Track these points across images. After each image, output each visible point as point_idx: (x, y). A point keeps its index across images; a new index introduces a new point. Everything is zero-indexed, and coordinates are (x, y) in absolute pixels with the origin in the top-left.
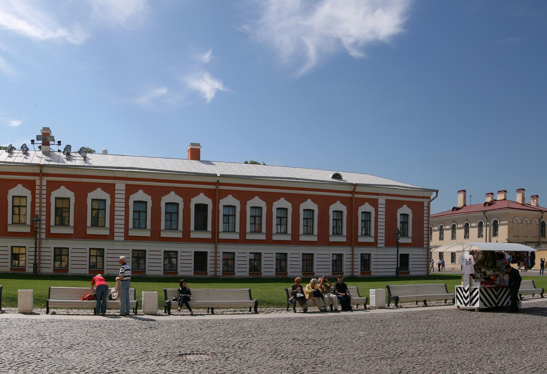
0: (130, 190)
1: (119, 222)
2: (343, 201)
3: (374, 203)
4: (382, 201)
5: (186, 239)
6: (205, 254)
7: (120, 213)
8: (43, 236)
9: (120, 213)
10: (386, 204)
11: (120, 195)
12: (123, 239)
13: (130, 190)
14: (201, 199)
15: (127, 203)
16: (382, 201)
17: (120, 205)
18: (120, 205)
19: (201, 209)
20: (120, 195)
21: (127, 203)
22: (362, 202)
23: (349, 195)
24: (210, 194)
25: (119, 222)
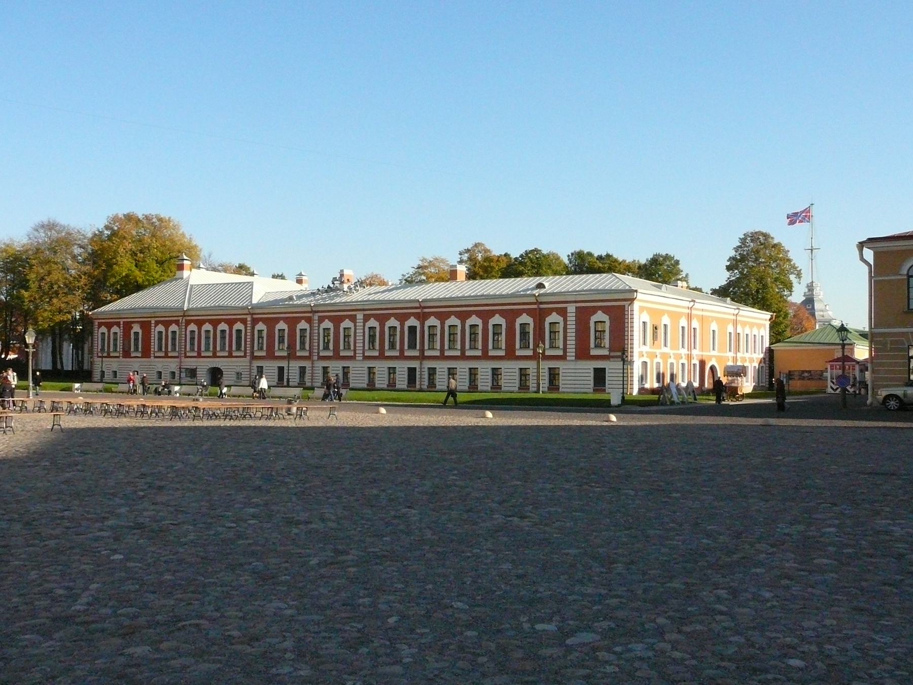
0: (366, 318)
1: (359, 345)
2: (529, 312)
3: (563, 312)
4: (571, 309)
5: (402, 357)
6: (415, 369)
7: (359, 338)
8: (315, 358)
9: (359, 338)
10: (576, 312)
11: (360, 324)
12: (361, 358)
13: (366, 318)
14: (412, 322)
15: (364, 329)
16: (571, 309)
17: (360, 331)
18: (360, 331)
19: (412, 329)
20: (360, 324)
21: (364, 329)
22: (549, 312)
23: (535, 306)
24: (417, 316)
25: (359, 345)
